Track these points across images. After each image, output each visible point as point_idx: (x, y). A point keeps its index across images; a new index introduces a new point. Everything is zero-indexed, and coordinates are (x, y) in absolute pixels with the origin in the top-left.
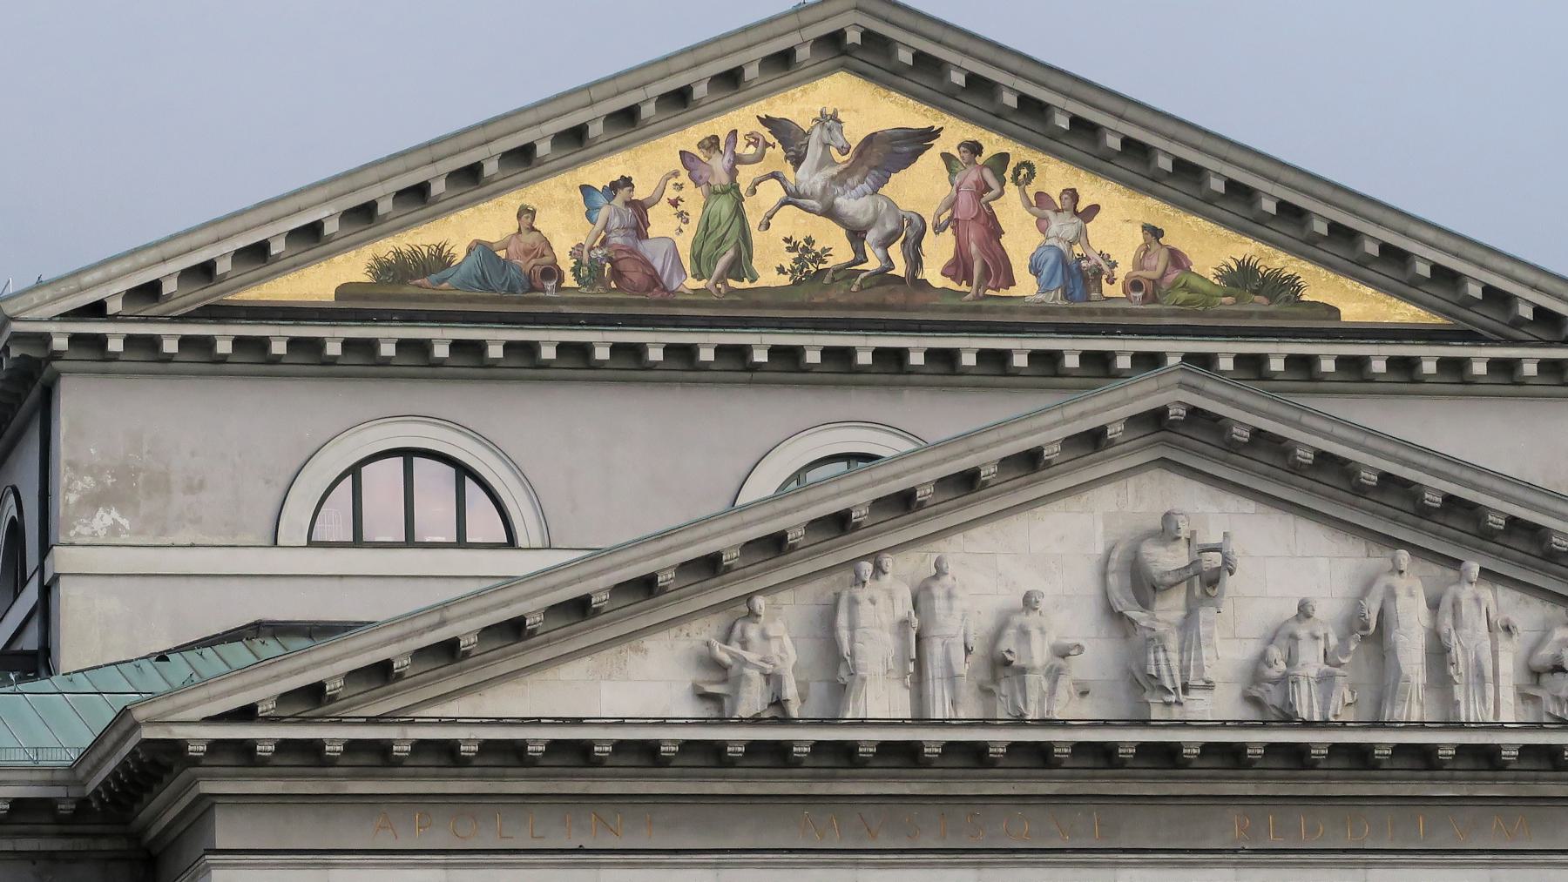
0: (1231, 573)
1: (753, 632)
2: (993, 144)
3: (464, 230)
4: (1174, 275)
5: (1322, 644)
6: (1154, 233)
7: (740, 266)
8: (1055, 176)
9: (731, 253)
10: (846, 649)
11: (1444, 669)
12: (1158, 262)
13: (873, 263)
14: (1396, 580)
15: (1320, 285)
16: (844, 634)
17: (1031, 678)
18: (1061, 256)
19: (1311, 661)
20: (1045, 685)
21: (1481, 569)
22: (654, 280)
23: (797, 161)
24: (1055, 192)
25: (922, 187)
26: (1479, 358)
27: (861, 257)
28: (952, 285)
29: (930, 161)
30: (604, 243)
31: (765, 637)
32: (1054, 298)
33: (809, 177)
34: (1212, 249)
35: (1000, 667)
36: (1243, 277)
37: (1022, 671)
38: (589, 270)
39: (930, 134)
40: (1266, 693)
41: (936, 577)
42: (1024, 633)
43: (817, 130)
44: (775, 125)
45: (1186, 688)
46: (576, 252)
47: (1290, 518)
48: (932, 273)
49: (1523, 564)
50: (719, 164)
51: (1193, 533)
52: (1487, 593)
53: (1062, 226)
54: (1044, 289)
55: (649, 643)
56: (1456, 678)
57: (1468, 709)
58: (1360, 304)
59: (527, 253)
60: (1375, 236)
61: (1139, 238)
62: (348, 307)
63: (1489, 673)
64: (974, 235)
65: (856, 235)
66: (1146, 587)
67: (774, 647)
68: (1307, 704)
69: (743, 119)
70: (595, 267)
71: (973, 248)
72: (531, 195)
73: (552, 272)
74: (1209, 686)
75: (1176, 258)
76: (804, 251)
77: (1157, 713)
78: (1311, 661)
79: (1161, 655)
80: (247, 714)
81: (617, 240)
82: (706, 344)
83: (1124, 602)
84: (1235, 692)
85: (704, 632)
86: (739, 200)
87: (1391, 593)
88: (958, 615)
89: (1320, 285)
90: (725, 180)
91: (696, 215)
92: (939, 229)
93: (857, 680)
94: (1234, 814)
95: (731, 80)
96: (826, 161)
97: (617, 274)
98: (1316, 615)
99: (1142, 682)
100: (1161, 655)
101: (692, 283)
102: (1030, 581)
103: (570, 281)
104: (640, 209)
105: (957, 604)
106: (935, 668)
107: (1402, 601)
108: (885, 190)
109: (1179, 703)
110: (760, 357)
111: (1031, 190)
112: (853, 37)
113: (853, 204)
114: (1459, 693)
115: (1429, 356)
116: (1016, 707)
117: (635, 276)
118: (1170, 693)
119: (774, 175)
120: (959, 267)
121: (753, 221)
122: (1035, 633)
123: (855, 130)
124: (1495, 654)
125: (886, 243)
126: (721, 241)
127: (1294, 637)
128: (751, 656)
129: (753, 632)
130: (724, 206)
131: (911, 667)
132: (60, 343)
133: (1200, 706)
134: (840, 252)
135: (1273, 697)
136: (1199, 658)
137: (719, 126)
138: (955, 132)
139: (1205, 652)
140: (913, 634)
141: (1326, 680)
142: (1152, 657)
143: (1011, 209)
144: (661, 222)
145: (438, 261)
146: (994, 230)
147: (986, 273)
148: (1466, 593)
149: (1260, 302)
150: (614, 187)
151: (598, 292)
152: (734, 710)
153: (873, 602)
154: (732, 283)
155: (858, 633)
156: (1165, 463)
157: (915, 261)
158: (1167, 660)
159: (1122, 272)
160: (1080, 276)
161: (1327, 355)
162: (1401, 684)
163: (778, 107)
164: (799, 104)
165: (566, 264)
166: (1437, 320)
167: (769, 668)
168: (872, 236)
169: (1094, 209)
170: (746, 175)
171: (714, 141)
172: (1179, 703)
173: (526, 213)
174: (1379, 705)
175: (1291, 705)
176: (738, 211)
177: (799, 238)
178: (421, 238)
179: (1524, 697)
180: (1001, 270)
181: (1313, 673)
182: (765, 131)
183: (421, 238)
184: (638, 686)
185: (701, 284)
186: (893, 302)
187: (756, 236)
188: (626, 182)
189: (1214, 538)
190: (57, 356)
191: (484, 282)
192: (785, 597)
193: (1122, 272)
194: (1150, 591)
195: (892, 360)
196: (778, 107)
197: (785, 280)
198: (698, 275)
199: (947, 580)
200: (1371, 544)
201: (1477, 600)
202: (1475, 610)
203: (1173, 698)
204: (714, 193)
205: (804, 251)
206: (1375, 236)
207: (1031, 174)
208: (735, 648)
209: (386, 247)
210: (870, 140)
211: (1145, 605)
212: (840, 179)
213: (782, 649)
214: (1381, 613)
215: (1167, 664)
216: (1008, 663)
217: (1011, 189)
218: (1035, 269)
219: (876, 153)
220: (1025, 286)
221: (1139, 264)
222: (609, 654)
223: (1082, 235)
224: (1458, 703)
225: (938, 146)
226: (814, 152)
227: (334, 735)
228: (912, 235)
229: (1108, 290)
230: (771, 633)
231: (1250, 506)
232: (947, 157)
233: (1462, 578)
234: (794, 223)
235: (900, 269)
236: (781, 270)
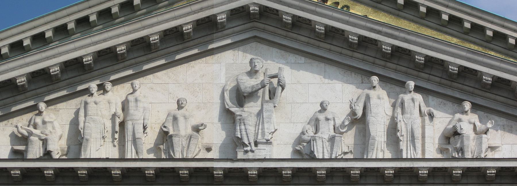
0: (283, 89)
1: (39, 120)
5: (332, 123)
10: (81, 125)
11: (395, 134)
14: (372, 93)
16: (81, 119)
17: (175, 140)
19: (327, 131)
20: (185, 143)
21: (415, 86)
31: (44, 123)
35: (165, 137)
37: (171, 136)
40: (303, 149)
41: (132, 93)
42: (175, 119)
45: (256, 144)
47: (322, 65)
49: (440, 84)
51: (266, 70)
52: (419, 97)
56: (401, 138)
57: (407, 153)
60: (491, 28)
63: (418, 133)
66: (241, 97)
67: (49, 127)
74: (268, 142)
77: (240, 155)
78: (327, 131)
79: (243, 127)
83: (230, 104)
85: (21, 123)
87: (368, 98)
88: (141, 110)
93: (84, 140)
98: (329, 108)
99: (237, 143)
100: (243, 127)
102: (181, 94)
105: (140, 104)
106: (129, 137)
107: (374, 101)
109: (252, 151)
114: (403, 145)
116: (170, 155)
118: (247, 146)
122: (181, 120)
124: (423, 127)
127: (317, 120)
128: (37, 132)
129: (39, 120)
131: (117, 136)
133: (262, 152)
136: (263, 129)
139: (266, 126)
140: (118, 121)
141: (332, 140)
142: (238, 128)
148: (407, 97)
152: (27, 156)
153: (96, 103)
155: (88, 118)
156: (255, 38)
158: (246, 129)
162: (371, 141)
167: (43, 137)
172: (252, 151)
174: (363, 154)
175: (312, 152)
179: (441, 150)
181: (326, 137)
189: (274, 72)
192: (61, 106)
194: (243, 98)
199: (137, 94)
200: (363, 77)
201: (413, 100)
202: (412, 104)
203: (249, 148)
206: (491, 28)
208: (31, 129)
213: (54, 128)
214: (365, 108)
215: (248, 130)
216: (167, 133)
224: (402, 150)
230: (47, 120)
231: (302, 59)
233: (407, 91)
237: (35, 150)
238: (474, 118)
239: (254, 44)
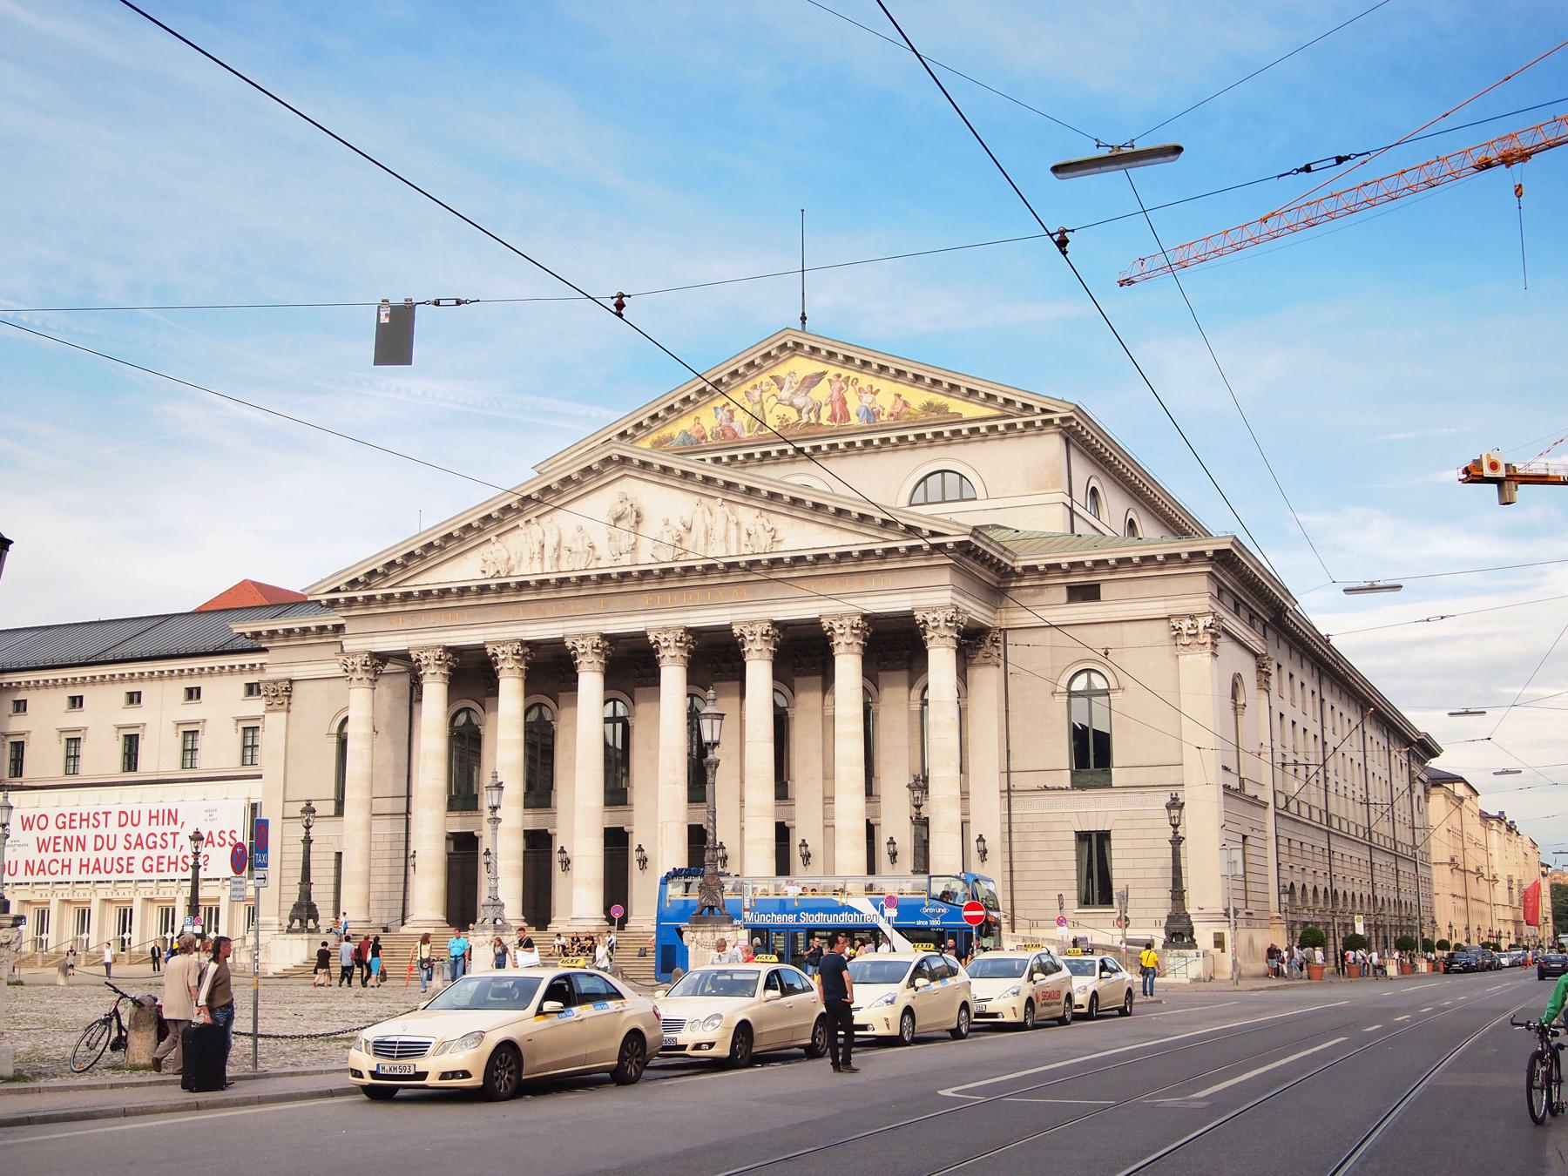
2: (845, 373)
8: (865, 380)
12: (900, 405)
13: (805, 420)
15: (956, 405)
22: (735, 435)
25: (822, 392)
29: (825, 381)
33: (785, 394)
34: (918, 398)
36: (929, 407)
38: (716, 435)
39: (825, 373)
48: (824, 421)
50: (757, 393)
52: (726, 508)
53: (867, 398)
55: (470, 555)
58: (970, 410)
61: (893, 398)
64: (838, 405)
65: (799, 411)
69: (765, 378)
72: (697, 413)
75: (906, 404)
76: (783, 419)
80: (337, 590)
89: (956, 405)
94: (646, 596)
101: (745, 435)
112: (790, 344)
113: (799, 401)
117: (729, 434)
120: (833, 417)
130: (758, 407)
133: (626, 560)
134: (794, 417)
137: (757, 381)
138: (832, 370)
143: (850, 395)
145: (671, 438)
146: (844, 403)
157: (818, 417)
160: (872, 414)
163: (777, 372)
164: (781, 371)
165: (708, 433)
166: (997, 413)
170: (765, 396)
178: (666, 432)
183: (666, 432)
184: (464, 570)
186: (812, 431)
193: (888, 410)
195: (800, 451)
196: (777, 372)
209: (654, 436)
219: (807, 383)
220: (855, 421)
222: (456, 561)
225: (827, 377)
226: (787, 385)
227: (359, 594)
234: (781, 410)
239: (626, 479)
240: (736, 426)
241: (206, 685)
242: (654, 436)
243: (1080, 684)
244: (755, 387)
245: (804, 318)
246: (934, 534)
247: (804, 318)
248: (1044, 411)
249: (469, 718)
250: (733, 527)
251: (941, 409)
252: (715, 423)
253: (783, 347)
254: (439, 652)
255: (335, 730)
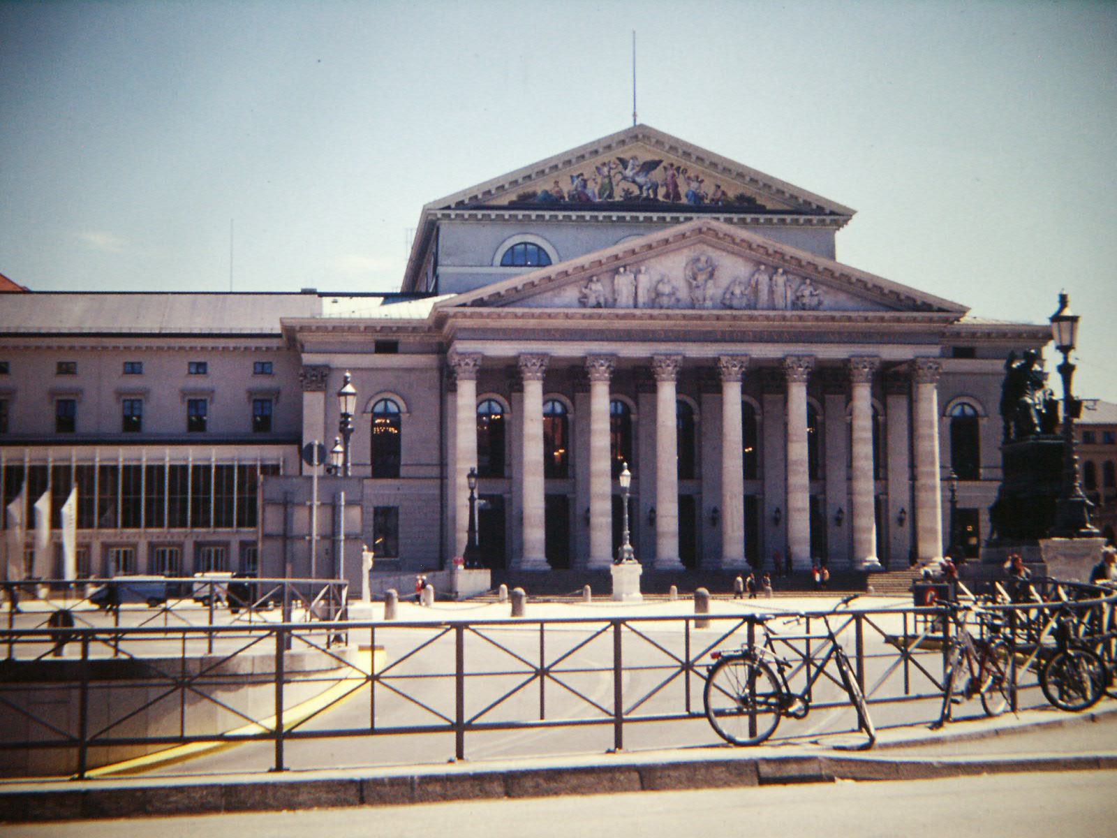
3: (541, 187)
4: (723, 197)
6: (718, 187)
7: (610, 196)
9: (608, 192)
12: (719, 193)
13: (645, 195)
18: (694, 193)
19: (737, 291)
22: (588, 199)
23: (626, 168)
24: (692, 175)
25: (657, 175)
26: (802, 218)
27: (641, 192)
28: (665, 200)
29: (660, 168)
30: (576, 190)
32: (692, 203)
33: (629, 173)
36: (741, 198)
38: (572, 197)
39: (661, 162)
43: (631, 161)
44: (621, 160)
46: (569, 193)
48: (660, 198)
50: (605, 170)
53: (694, 185)
54: (689, 200)
59: (558, 192)
62: (512, 206)
65: (641, 187)
68: (735, 303)
70: (573, 196)
71: (671, 190)
73: (563, 197)
75: (724, 193)
76: (627, 192)
80: (464, 305)
81: (580, 189)
82: (601, 215)
84: (719, 301)
86: (610, 179)
90: (607, 173)
91: (599, 180)
92: (662, 186)
95: (609, 147)
96: (633, 169)
97: (579, 197)
101: (597, 200)
103: (567, 199)
104: (585, 181)
108: (649, 176)
110: (614, 219)
111: (686, 176)
112: (640, 136)
113: (640, 179)
115: (788, 218)
119: (620, 172)
120: (667, 196)
121: (614, 184)
123: (641, 161)
125: (648, 189)
126: (605, 190)
130: (606, 181)
132: (439, 216)
134: (637, 192)
135: (728, 302)
143: (681, 181)
144: (590, 185)
145: (534, 195)
146: (676, 186)
147: (674, 197)
149: (746, 204)
150: (578, 176)
151: (574, 202)
154: (609, 200)
157: (656, 194)
159: (709, 197)
160: (698, 198)
161: (762, 218)
163: (622, 156)
165: (566, 195)
168: (645, 188)
169: (702, 181)
170: (612, 172)
171: (604, 164)
173: (556, 183)
176: (610, 182)
177: (626, 188)
178: (530, 190)
180: (677, 196)
182: (618, 162)
185: (601, 200)
187: (615, 187)
188: (582, 174)
190: (438, 219)
191: (545, 199)
193: (709, 197)
197: (622, 199)
198: (600, 198)
204: (605, 177)
205: (627, 192)
207: (686, 172)
210: (645, 164)
211: (695, 279)
212: (637, 174)
215: (698, 293)
217: (681, 176)
218: (687, 196)
220: (684, 201)
221: (714, 195)
223: (699, 187)
225: (664, 164)
226: (630, 167)
228: (655, 187)
229: (707, 201)
232: (665, 168)
234: (625, 185)
235: (652, 196)
236: (621, 196)
237: (592, 301)
238: (811, 289)
240: (589, 192)
241: (149, 363)
242: (521, 191)
243: (957, 412)
244: (604, 164)
245: (635, 115)
246: (940, 310)
247: (635, 115)
248: (832, 213)
249: (386, 406)
250: (788, 289)
251: (751, 201)
252: (572, 187)
253: (636, 137)
254: (546, 361)
255: (369, 409)
